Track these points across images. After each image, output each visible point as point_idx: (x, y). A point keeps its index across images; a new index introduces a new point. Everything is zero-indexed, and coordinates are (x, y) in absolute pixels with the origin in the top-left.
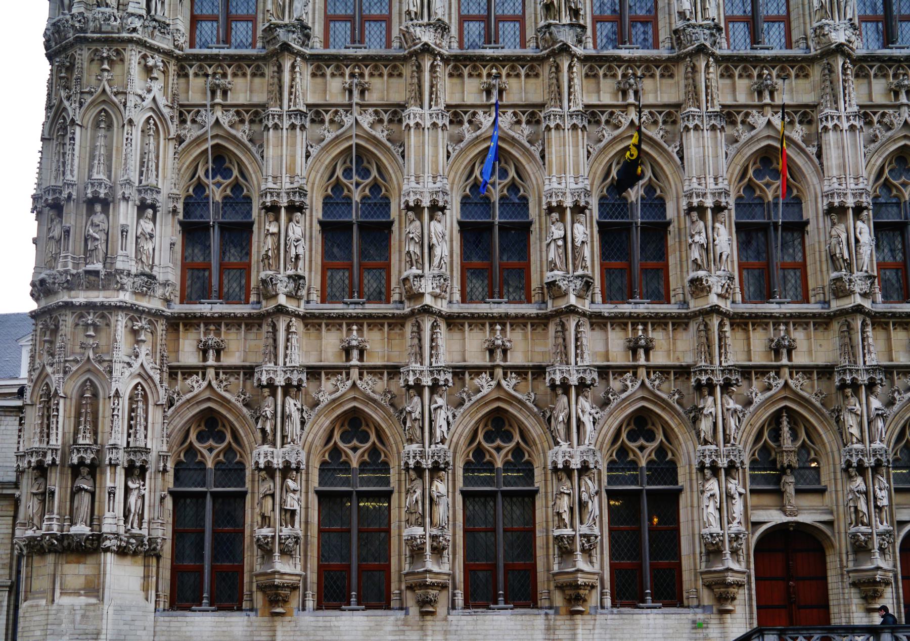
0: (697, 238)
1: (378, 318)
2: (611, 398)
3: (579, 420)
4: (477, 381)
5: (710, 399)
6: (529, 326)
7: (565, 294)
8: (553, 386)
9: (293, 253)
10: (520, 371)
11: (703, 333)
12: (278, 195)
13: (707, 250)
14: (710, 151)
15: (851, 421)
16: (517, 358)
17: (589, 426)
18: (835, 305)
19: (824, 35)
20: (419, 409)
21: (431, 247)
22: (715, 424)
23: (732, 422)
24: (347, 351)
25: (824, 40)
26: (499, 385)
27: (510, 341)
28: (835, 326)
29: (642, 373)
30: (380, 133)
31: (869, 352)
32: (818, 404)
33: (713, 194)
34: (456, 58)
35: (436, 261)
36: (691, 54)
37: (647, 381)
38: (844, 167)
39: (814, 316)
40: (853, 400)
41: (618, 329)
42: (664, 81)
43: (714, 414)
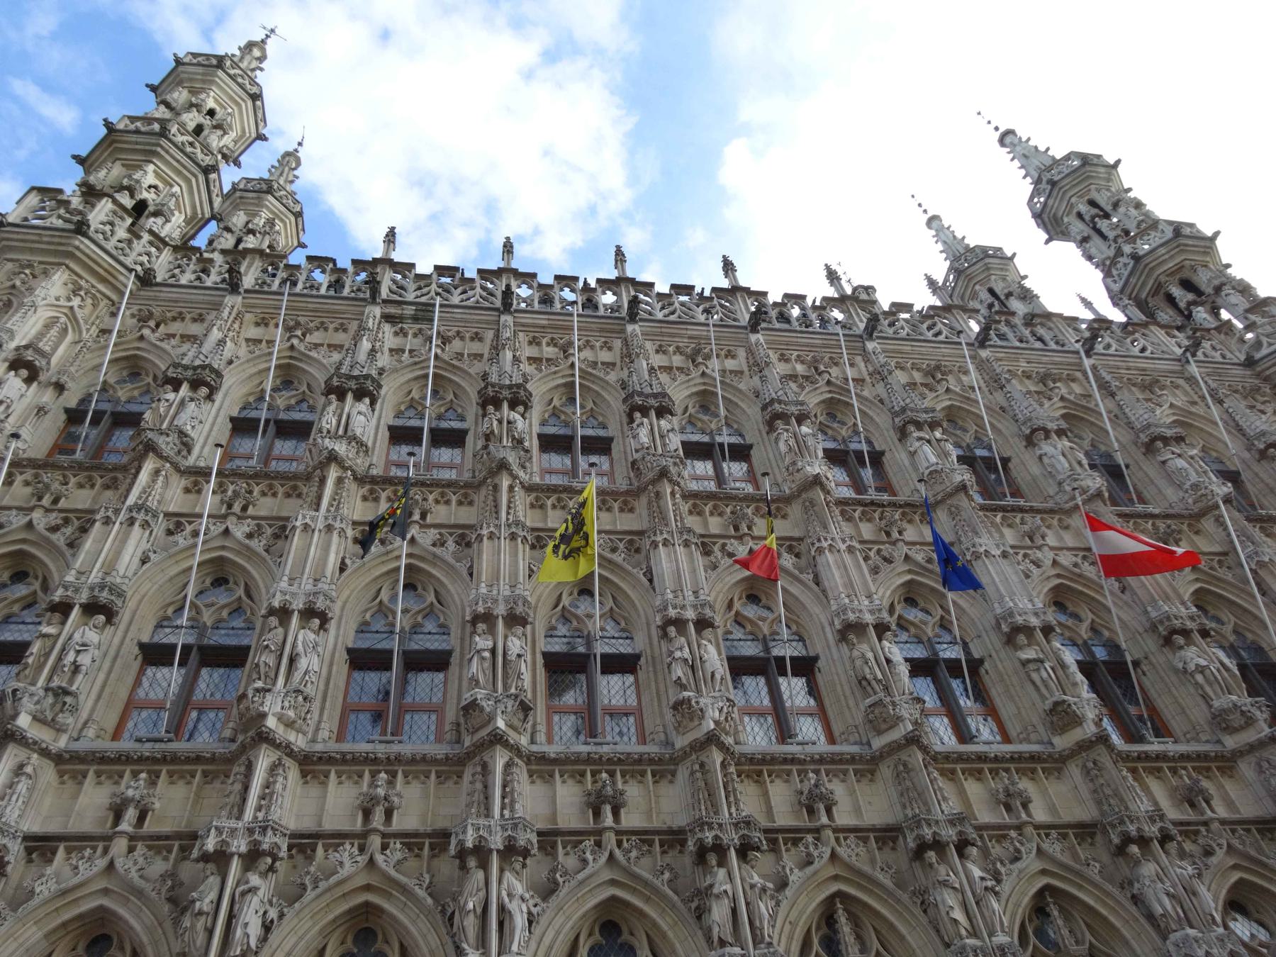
0: (678, 654)
1: (188, 760)
2: (561, 880)
3: (502, 909)
4: (334, 856)
5: (722, 873)
6: (433, 776)
7: (491, 718)
8: (462, 854)
9: (71, 657)
10: (411, 841)
11: (699, 775)
12: (77, 590)
13: (692, 667)
14: (684, 566)
15: (950, 899)
16: (406, 821)
17: (520, 921)
18: (878, 743)
19: (798, 471)
20: (213, 896)
21: (292, 660)
22: (734, 911)
23: (763, 908)
24: (118, 813)
25: (798, 476)
26: (371, 861)
27: (399, 795)
28: (885, 770)
29: (610, 839)
30: (258, 545)
31: (945, 799)
32: (888, 882)
33: (695, 607)
34: (374, 480)
35: (297, 676)
36: (653, 482)
37: (617, 852)
38: (849, 584)
39: (853, 759)
40: (942, 870)
41: (570, 782)
42: (624, 515)
43: (730, 894)
